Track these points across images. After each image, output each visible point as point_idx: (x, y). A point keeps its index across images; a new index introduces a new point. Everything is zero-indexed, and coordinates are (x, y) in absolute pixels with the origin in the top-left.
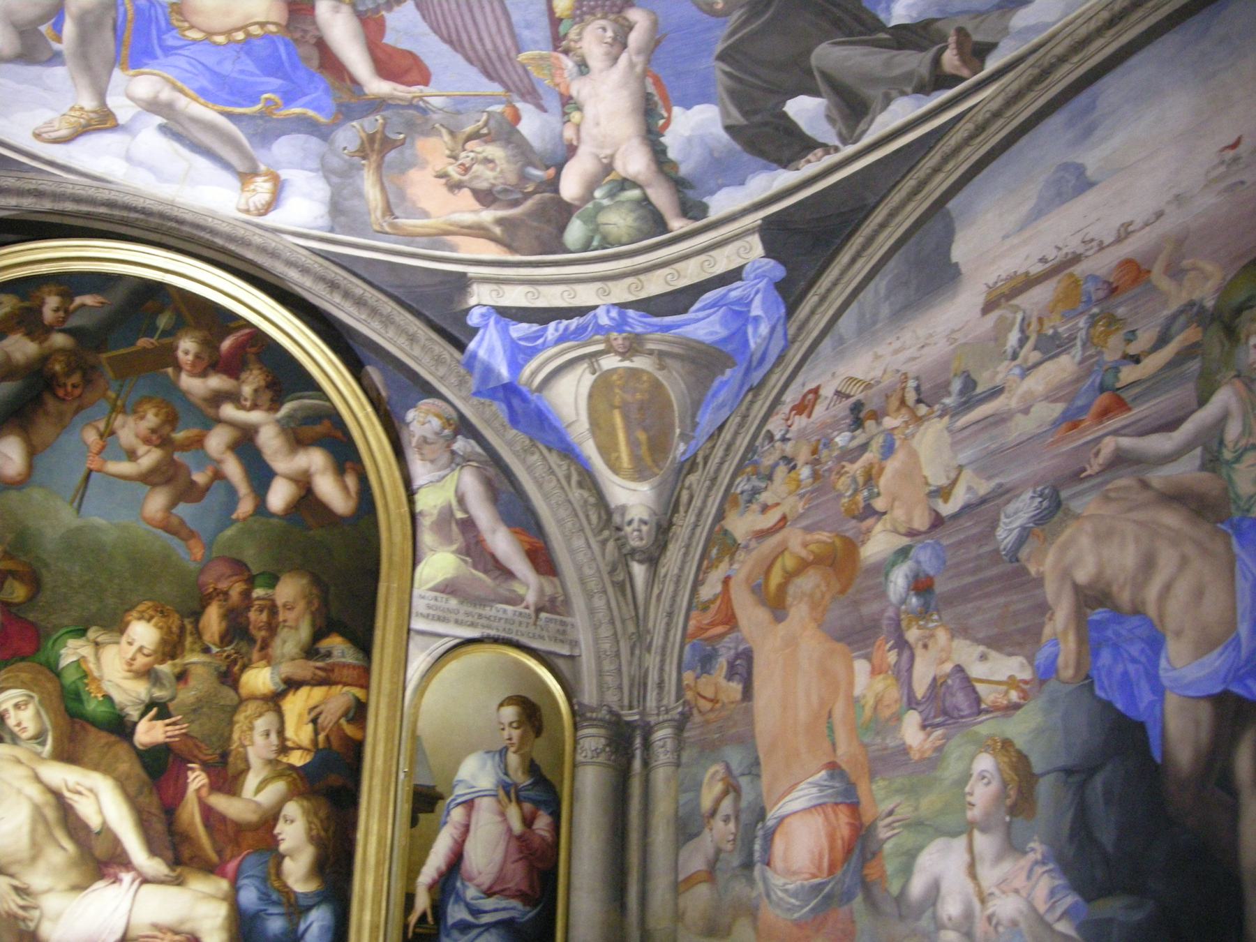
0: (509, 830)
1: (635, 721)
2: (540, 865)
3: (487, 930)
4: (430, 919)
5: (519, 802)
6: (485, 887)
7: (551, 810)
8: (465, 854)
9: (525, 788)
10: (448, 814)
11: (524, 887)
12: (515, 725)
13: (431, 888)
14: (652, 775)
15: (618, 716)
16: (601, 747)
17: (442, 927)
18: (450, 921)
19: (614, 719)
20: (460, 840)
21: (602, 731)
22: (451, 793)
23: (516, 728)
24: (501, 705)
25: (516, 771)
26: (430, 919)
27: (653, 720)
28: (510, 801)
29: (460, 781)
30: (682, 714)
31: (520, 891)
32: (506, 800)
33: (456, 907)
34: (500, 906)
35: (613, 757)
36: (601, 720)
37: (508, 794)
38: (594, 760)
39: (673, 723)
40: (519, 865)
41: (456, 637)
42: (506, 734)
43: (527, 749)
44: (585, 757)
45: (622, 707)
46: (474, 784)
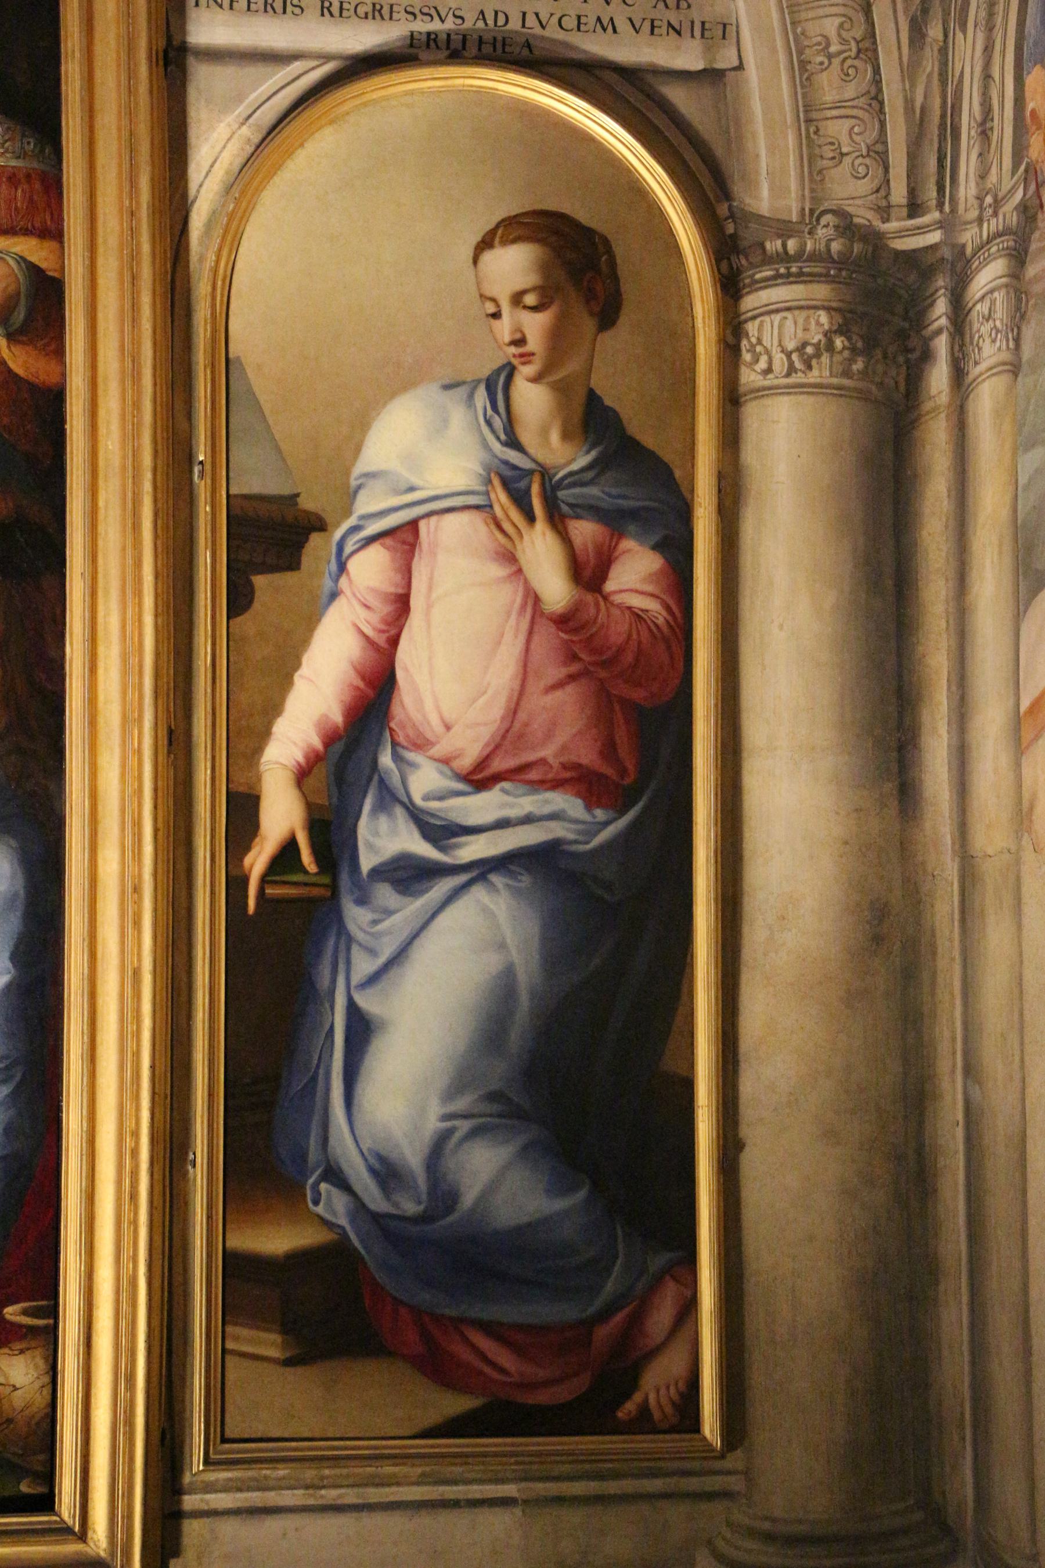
0: (533, 599)
1: (933, 247)
2: (638, 695)
3: (482, 878)
4: (306, 857)
5: (557, 520)
6: (466, 762)
7: (655, 538)
8: (400, 674)
9: (575, 479)
10: (342, 568)
11: (587, 755)
12: (530, 299)
13: (302, 775)
14: (971, 406)
15: (874, 239)
16: (817, 337)
17: (344, 879)
18: (367, 862)
19: (857, 248)
20: (381, 640)
21: (821, 291)
22: (348, 512)
23: (534, 309)
24: (486, 244)
25: (544, 432)
26: (306, 857)
27: (969, 237)
28: (531, 519)
29: (368, 475)
30: (1024, 208)
31: (577, 766)
32: (515, 515)
33: (383, 822)
34: (513, 813)
35: (858, 365)
36: (814, 257)
37: (521, 501)
38: (798, 378)
39: (1008, 241)
40: (568, 696)
41: (326, 57)
42: (504, 329)
43: (572, 367)
44: (769, 370)
45: (885, 212)
46: (416, 481)
